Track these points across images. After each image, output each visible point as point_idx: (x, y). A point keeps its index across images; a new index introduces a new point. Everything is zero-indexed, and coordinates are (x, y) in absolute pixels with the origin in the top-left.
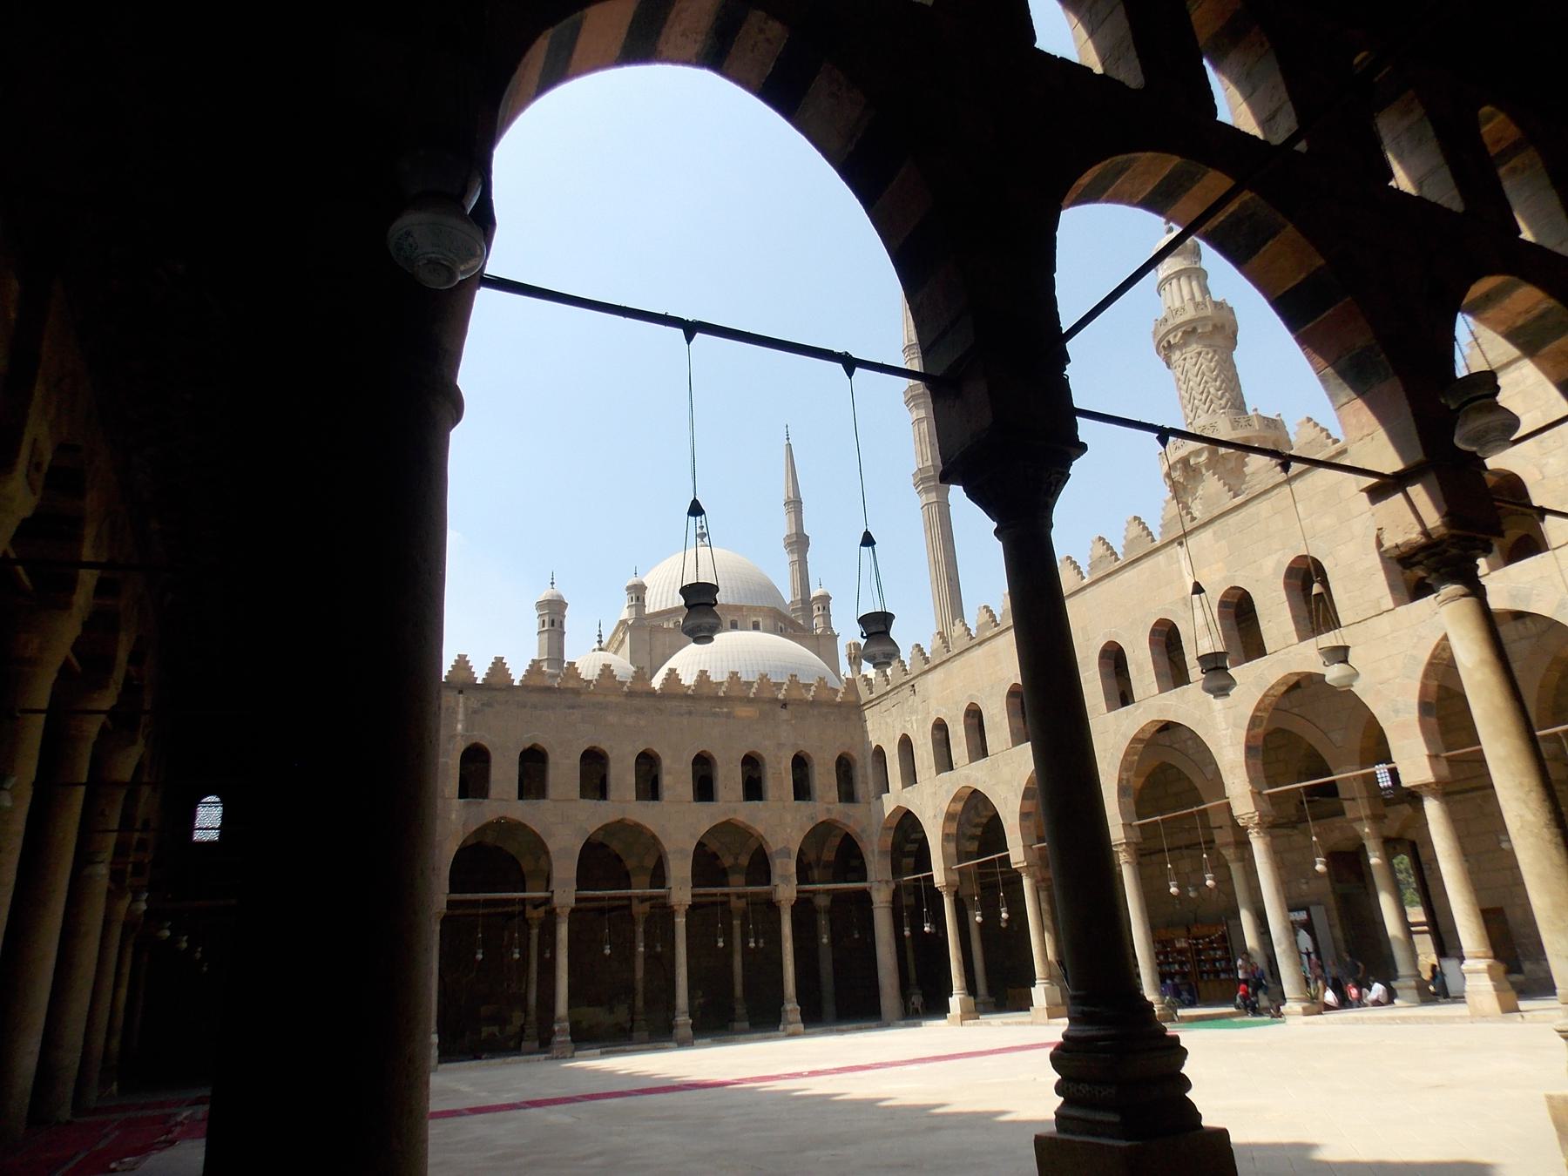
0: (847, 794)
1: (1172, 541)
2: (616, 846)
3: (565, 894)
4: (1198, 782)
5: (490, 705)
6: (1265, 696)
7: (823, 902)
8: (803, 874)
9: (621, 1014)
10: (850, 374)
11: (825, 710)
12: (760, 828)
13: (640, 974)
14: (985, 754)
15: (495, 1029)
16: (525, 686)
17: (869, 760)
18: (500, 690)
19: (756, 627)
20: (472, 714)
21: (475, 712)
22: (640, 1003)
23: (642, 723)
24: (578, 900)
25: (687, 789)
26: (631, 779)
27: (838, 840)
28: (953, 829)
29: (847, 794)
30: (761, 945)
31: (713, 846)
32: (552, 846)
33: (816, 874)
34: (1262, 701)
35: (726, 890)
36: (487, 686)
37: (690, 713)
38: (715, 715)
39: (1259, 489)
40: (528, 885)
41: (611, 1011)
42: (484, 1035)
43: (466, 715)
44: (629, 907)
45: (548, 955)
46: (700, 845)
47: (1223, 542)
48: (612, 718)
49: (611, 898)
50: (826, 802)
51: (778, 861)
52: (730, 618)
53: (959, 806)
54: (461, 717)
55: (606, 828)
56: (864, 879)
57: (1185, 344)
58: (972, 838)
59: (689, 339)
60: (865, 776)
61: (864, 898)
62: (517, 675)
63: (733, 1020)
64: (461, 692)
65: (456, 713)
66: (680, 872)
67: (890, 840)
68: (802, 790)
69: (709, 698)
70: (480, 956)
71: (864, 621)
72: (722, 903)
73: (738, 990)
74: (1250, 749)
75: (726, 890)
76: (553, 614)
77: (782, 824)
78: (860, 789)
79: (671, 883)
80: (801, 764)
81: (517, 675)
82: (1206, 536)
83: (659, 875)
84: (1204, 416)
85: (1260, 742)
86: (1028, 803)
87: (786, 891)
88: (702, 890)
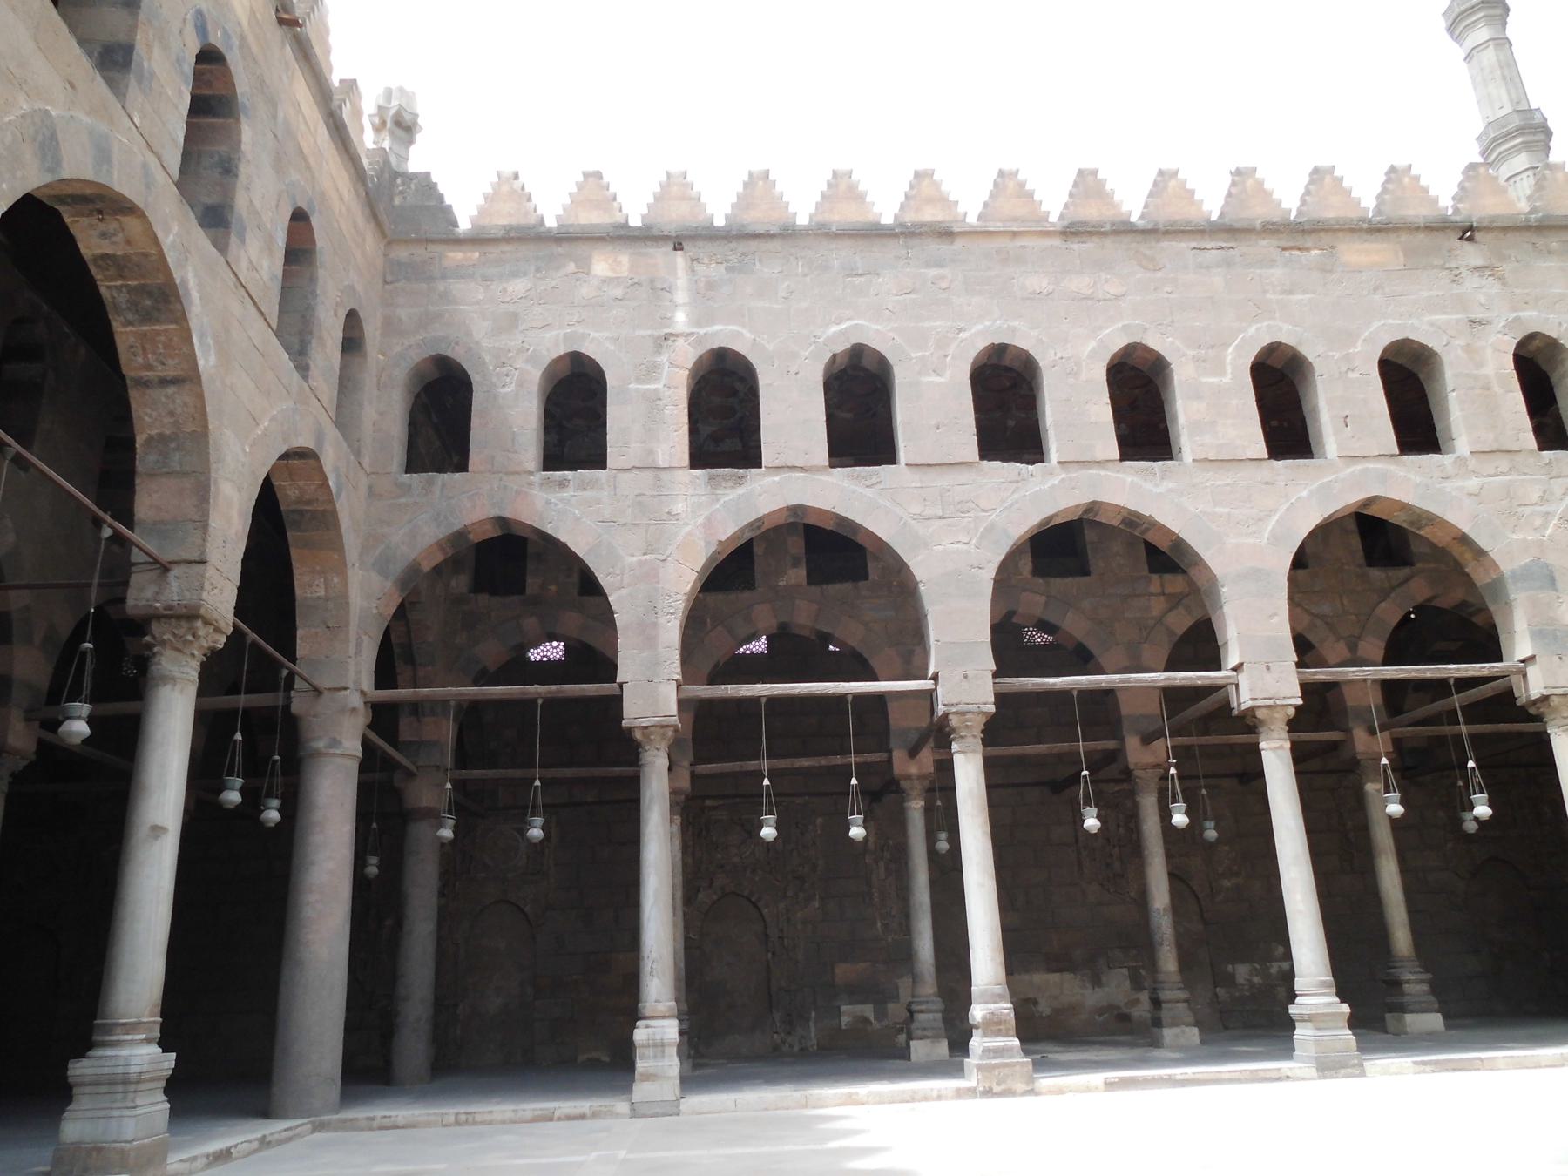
9: (1116, 987)
12: (1460, 519)
13: (1160, 894)
15: (868, 1010)
18: (767, 236)
20: (704, 292)
22: (1168, 961)
26: (1101, 412)
32: (921, 566)
37: (1228, 264)
41: (1097, 982)
42: (845, 1020)
45: (943, 846)
48: (1037, 282)
54: (681, 296)
63: (1402, 1009)
64: (678, 247)
70: (768, 833)
73: (1402, 938)
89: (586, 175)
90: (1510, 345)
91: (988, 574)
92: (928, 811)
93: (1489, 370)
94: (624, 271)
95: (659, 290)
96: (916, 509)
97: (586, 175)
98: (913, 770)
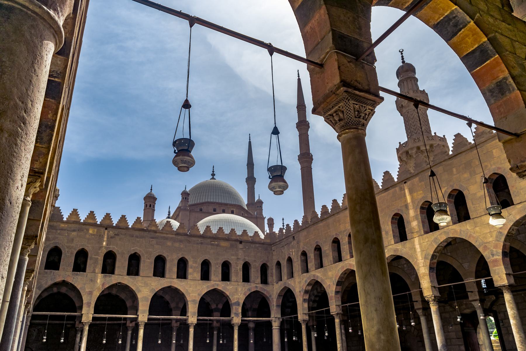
0: (264, 281)
1: (402, 181)
2: (167, 297)
3: (143, 317)
4: (408, 282)
5: (118, 235)
6: (438, 246)
7: (251, 325)
8: (244, 313)
10: (271, 54)
11: (257, 245)
12: (228, 293)
14: (322, 266)
16: (133, 228)
17: (274, 267)
19: (232, 213)
20: (110, 238)
21: (112, 237)
23: (182, 246)
24: (149, 319)
25: (198, 275)
27: (259, 300)
28: (307, 297)
29: (264, 281)
30: (225, 342)
31: (208, 299)
33: (250, 313)
34: (436, 248)
35: (212, 318)
36: (117, 227)
37: (202, 243)
38: (212, 245)
39: (438, 161)
40: (129, 312)
43: (108, 238)
44: (170, 324)
45: (134, 343)
46: (202, 299)
47: (423, 183)
48: (169, 244)
49: (163, 319)
50: (255, 284)
51: (234, 307)
52: (222, 208)
53: (310, 288)
54: (105, 239)
55: (163, 289)
56: (270, 317)
57: (408, 106)
58: (314, 301)
59: (191, 26)
60: (272, 273)
61: (269, 324)
62: (131, 223)
64: (106, 229)
65: (103, 237)
66: (192, 309)
67: (281, 302)
68: (246, 278)
69: (210, 238)
71: (271, 170)
72: (210, 324)
74: (431, 269)
75: (212, 318)
76: (150, 202)
77: (237, 292)
78: (270, 279)
79: (189, 314)
80: (246, 267)
81: (131, 223)
82: (416, 179)
83: (184, 311)
84: (415, 135)
85: (435, 266)
86: (338, 287)
87: (237, 320)
88: (201, 318)
89: (91, 212)
90: (242, 263)
91: (150, 298)
92: (132, 334)
93: (238, 268)
94: (95, 233)
95: (101, 237)
96: (140, 284)
97: (91, 212)
98: (131, 325)
